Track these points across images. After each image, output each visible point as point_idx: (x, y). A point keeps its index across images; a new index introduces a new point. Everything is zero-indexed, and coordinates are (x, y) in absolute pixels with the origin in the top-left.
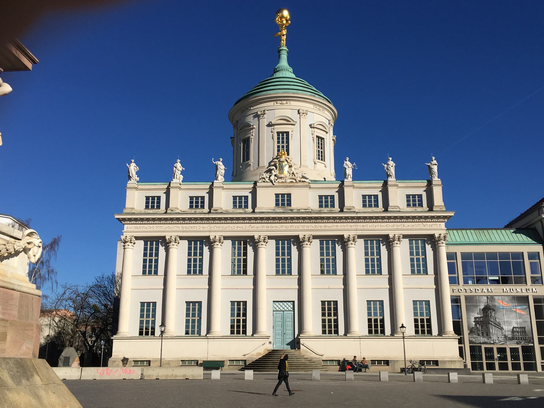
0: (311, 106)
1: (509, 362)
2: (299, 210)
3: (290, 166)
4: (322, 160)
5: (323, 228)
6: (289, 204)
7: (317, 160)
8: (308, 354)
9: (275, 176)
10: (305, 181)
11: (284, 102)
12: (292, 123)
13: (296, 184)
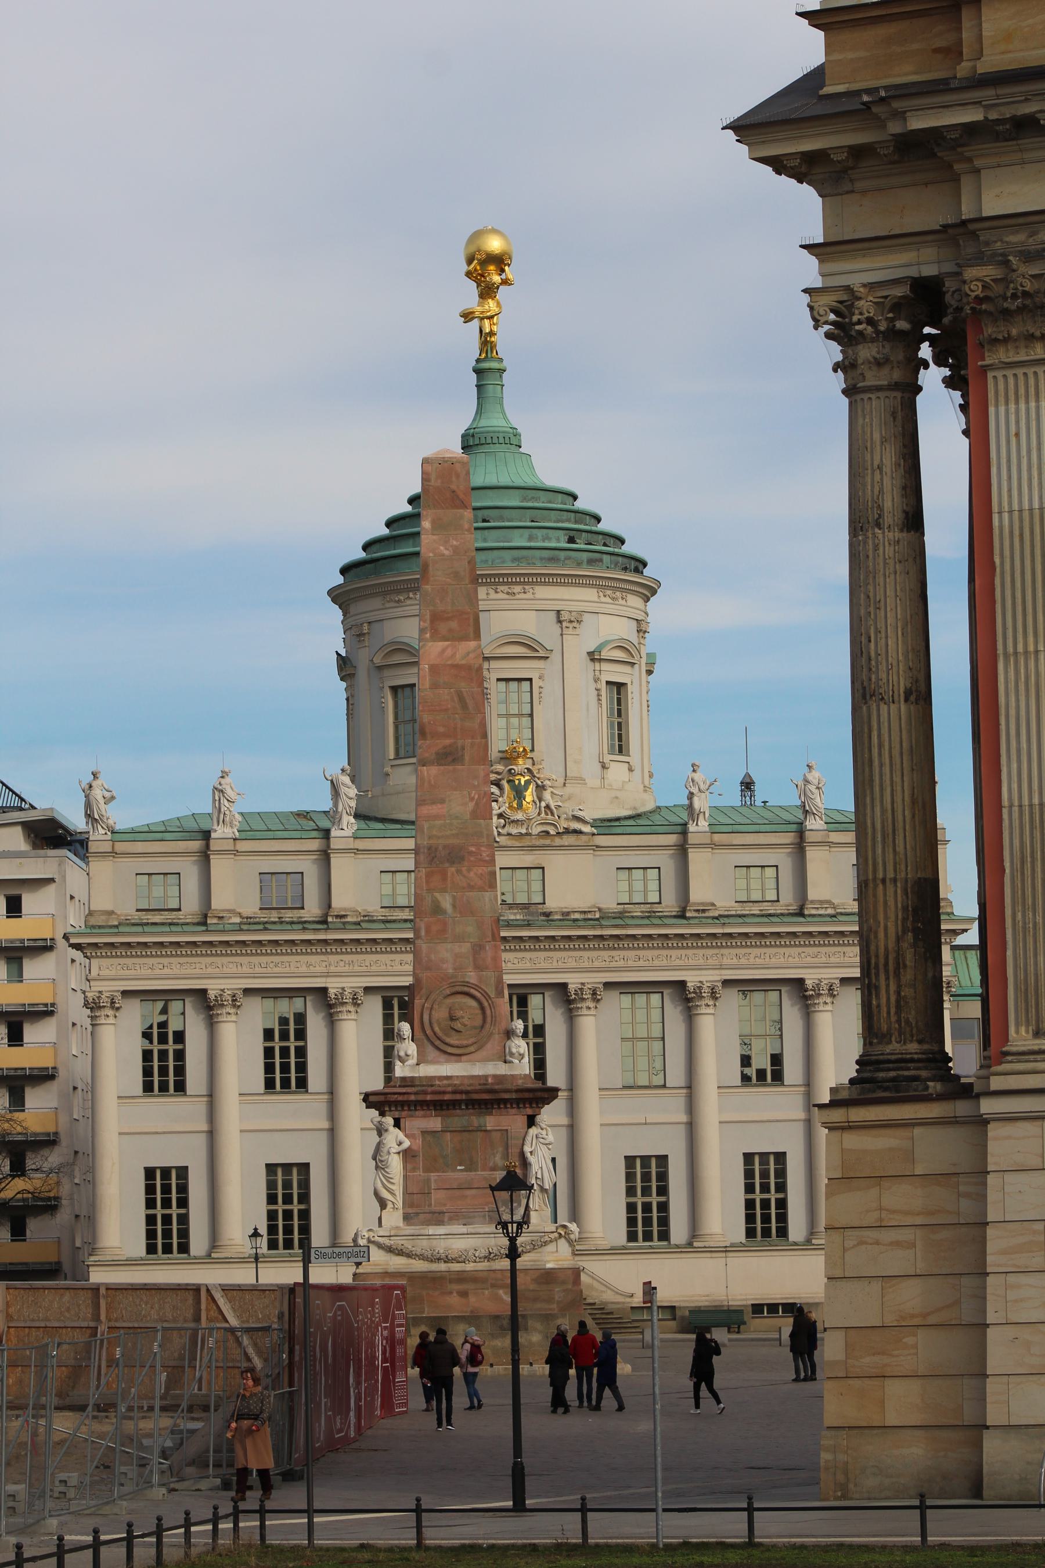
0: (590, 594)
2: (568, 913)
3: (540, 788)
4: (620, 751)
5: (630, 963)
7: (607, 758)
8: (594, 1294)
9: (500, 816)
10: (581, 832)
11: (517, 589)
12: (542, 654)
13: (558, 841)
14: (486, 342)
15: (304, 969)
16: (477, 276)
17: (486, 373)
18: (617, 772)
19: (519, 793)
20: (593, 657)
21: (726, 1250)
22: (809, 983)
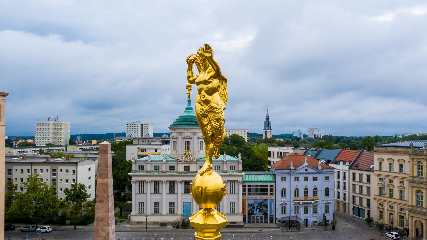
1: (260, 220)
6: (189, 169)
14: (189, 97)
16: (187, 88)
17: (189, 101)
18: (201, 152)
19: (187, 156)
20: (198, 138)
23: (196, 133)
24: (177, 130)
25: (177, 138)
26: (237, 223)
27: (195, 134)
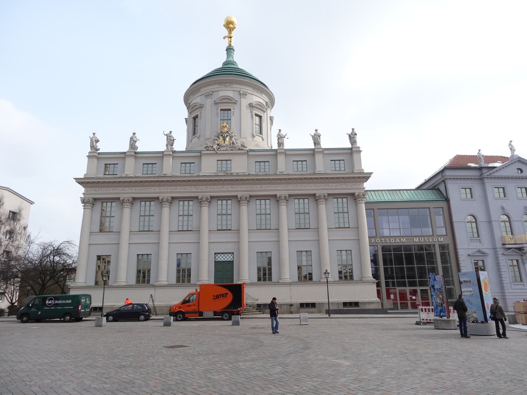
3: (231, 138)
4: (260, 134)
15: (152, 191)
18: (258, 139)
19: (224, 139)
20: (251, 106)
21: (290, 284)
22: (317, 195)
23: (245, 94)
24: (202, 90)
25: (201, 107)
26: (365, 303)
27: (243, 95)
